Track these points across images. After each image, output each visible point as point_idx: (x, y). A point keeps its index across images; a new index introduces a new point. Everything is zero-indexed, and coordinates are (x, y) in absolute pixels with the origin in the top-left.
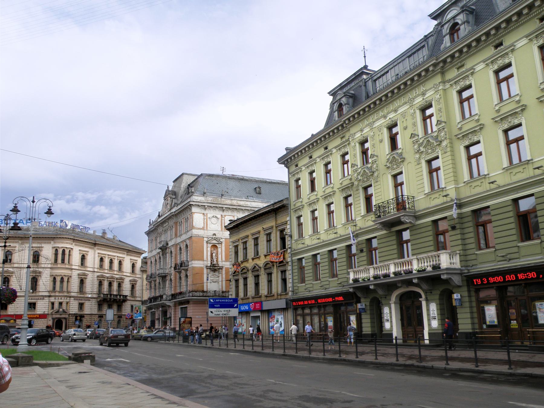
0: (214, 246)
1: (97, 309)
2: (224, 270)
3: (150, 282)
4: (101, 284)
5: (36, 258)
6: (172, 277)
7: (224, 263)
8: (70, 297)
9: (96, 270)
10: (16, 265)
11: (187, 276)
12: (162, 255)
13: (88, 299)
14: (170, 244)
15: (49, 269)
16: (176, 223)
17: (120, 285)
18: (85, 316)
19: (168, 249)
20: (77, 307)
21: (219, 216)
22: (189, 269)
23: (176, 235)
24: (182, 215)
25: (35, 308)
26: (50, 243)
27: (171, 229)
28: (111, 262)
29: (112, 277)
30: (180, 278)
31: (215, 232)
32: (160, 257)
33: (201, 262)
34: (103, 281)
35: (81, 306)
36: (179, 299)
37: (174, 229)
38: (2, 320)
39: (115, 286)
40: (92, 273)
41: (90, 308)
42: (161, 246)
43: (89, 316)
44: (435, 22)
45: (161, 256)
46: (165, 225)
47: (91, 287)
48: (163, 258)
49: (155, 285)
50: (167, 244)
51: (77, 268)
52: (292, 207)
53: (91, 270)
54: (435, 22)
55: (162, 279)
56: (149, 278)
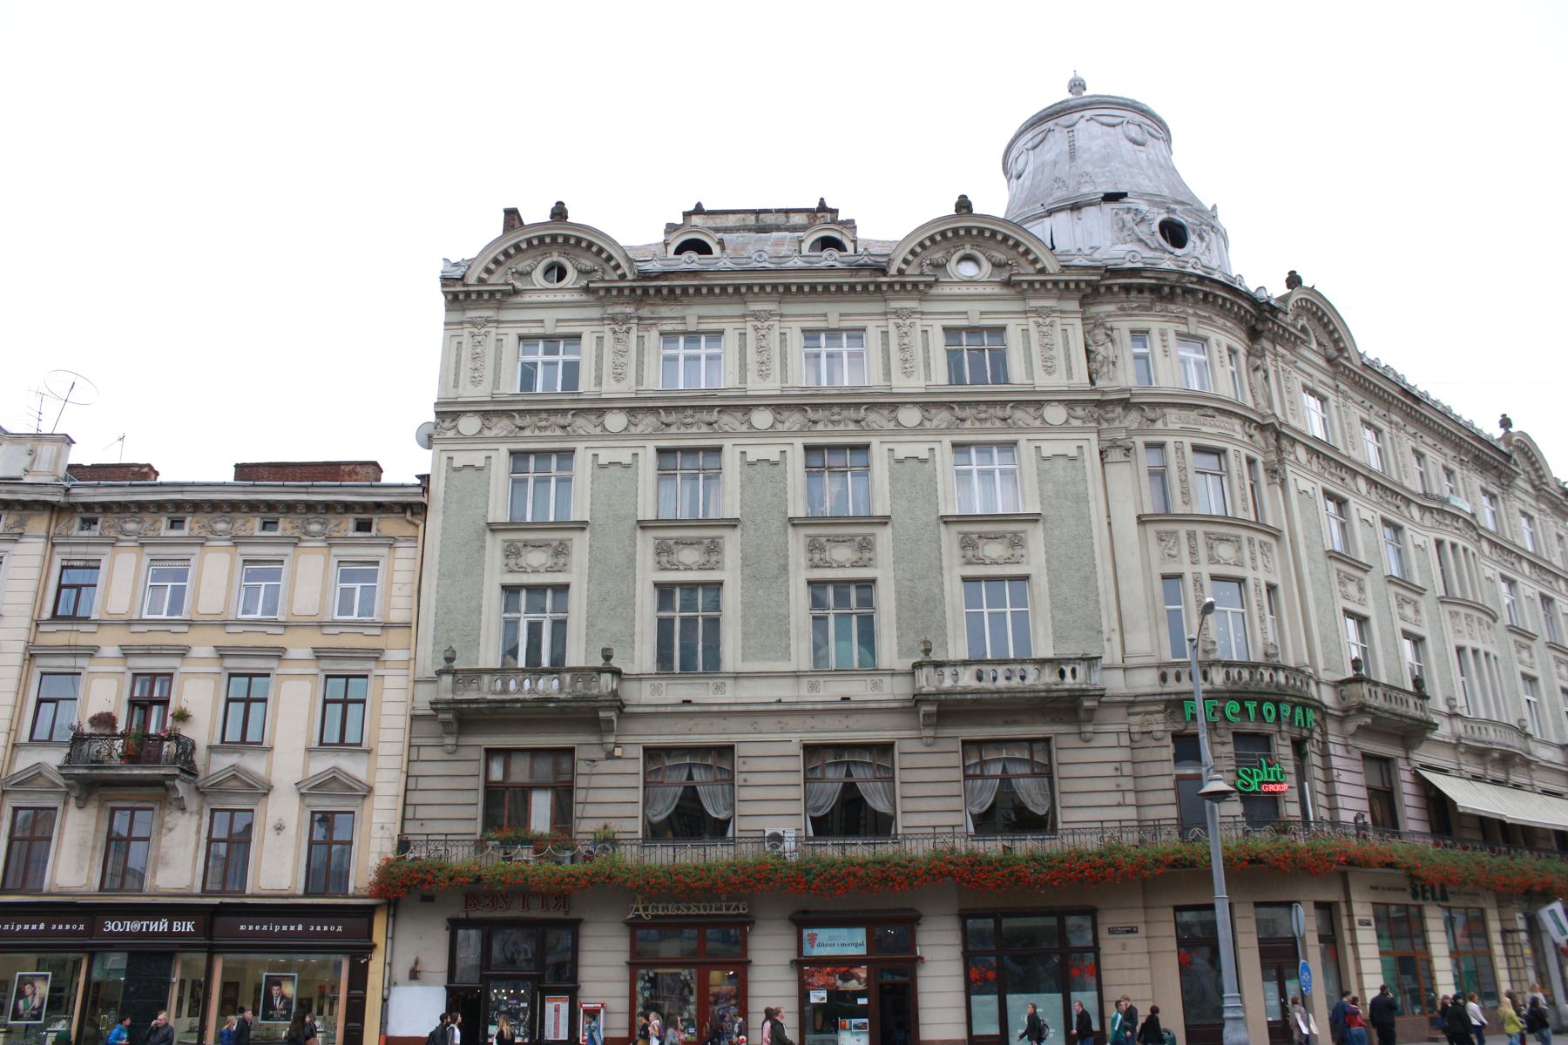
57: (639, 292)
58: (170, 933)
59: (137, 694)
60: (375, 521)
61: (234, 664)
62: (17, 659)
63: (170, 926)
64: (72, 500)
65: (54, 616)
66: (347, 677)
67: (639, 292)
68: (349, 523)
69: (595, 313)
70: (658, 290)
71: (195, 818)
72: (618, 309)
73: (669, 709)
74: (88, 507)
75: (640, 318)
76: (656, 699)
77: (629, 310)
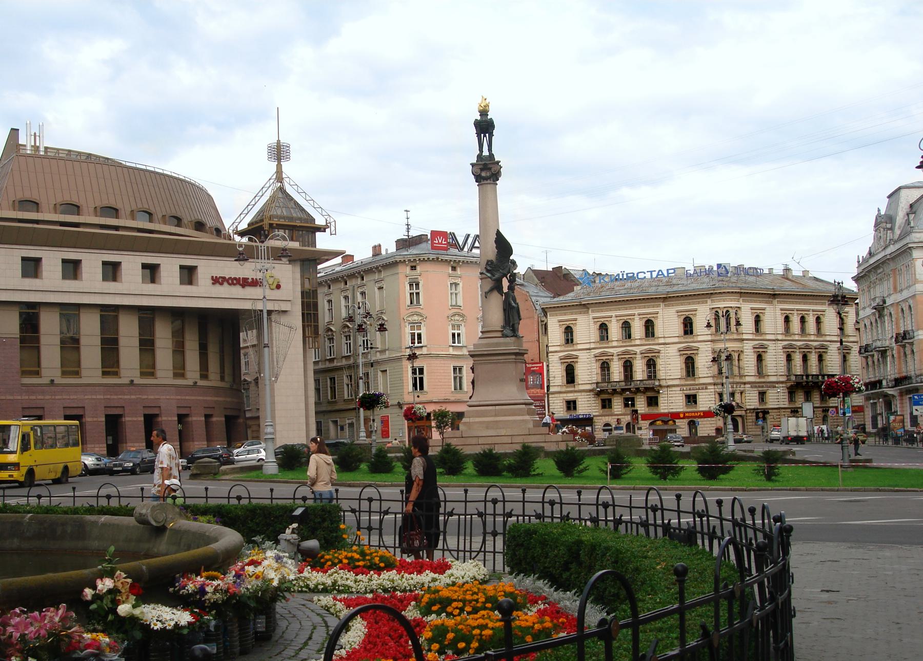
1: (787, 400)
3: (867, 358)
4: (789, 358)
5: (688, 326)
6: (894, 352)
8: (745, 383)
9: (780, 337)
10: (662, 341)
11: (913, 351)
12: (879, 317)
13: (773, 385)
14: (889, 302)
15: (709, 343)
16: (894, 270)
17: (821, 359)
18: (770, 411)
19: (886, 310)
20: (756, 398)
22: (914, 343)
23: (895, 289)
24: (902, 260)
25: (695, 402)
26: (707, 303)
27: (888, 280)
28: (803, 320)
29: (807, 347)
32: (876, 320)
34: (792, 354)
35: (762, 395)
36: (905, 385)
37: (891, 279)
38: (658, 420)
39: (813, 359)
40: (774, 342)
41: (777, 398)
42: (876, 304)
43: (776, 411)
45: (878, 319)
46: (879, 271)
47: (775, 363)
48: (881, 321)
49: (873, 362)
50: (884, 302)
51: (750, 337)
53: (772, 337)
55: (882, 355)
56: (863, 351)
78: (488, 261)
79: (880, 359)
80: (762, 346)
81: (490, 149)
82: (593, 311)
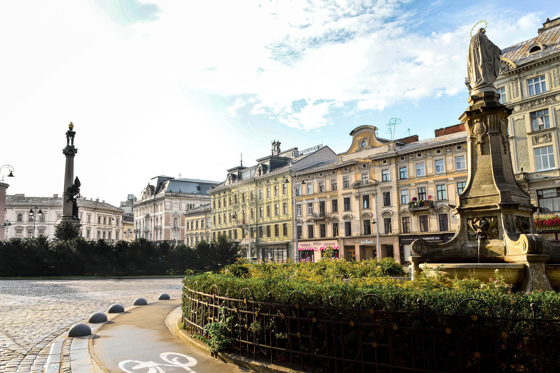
0: (176, 219)
2: (180, 230)
4: (99, 233)
7: (180, 227)
9: (96, 224)
10: (48, 223)
11: (161, 233)
21: (179, 203)
28: (105, 219)
29: (106, 229)
30: (157, 234)
31: (176, 211)
32: (143, 221)
33: (169, 226)
44: (258, 163)
46: (147, 204)
51: (85, 224)
52: (212, 212)
53: (94, 224)
54: (258, 163)
57: (518, 71)
58: (435, 240)
59: (419, 192)
60: (462, 146)
61: (437, 183)
62: (396, 189)
63: (435, 238)
64: (398, 155)
65: (401, 179)
66: (462, 183)
67: (518, 71)
68: (456, 147)
69: (507, 79)
70: (523, 69)
71: (436, 216)
72: (513, 77)
73: (541, 180)
74: (401, 155)
75: (520, 78)
76: (537, 178)
77: (517, 76)
78: (69, 188)
79: (144, 235)
80: (90, 228)
81: (72, 143)
82: (15, 208)
